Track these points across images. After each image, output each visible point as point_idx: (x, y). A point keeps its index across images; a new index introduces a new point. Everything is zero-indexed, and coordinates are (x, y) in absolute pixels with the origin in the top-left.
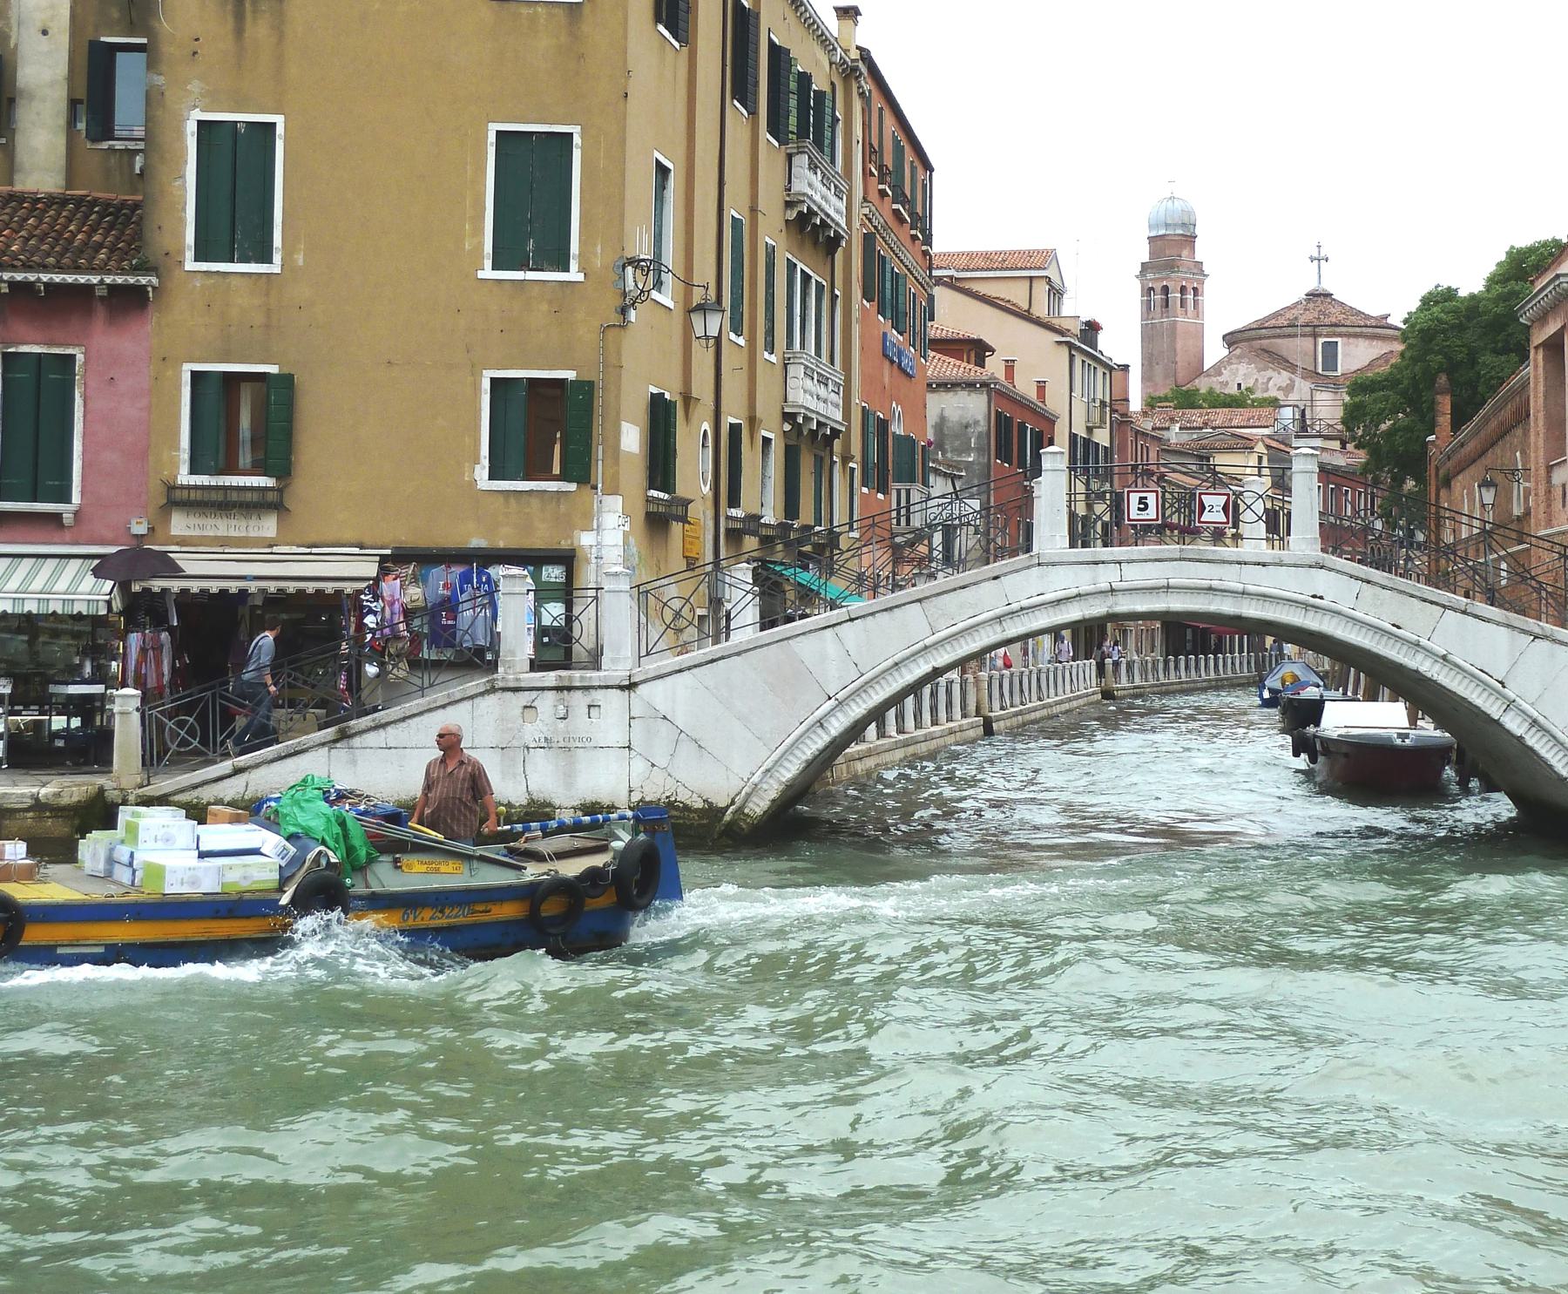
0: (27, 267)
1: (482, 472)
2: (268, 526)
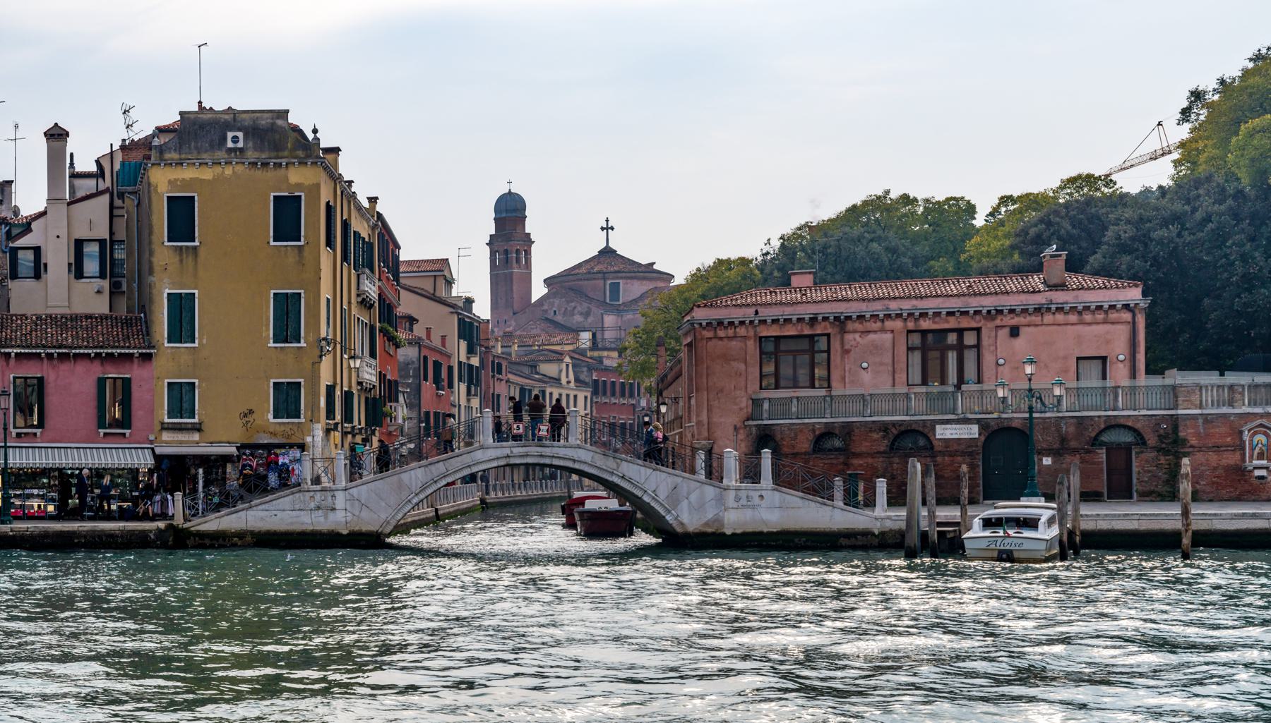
0: (113, 347)
1: (270, 416)
2: (196, 437)
